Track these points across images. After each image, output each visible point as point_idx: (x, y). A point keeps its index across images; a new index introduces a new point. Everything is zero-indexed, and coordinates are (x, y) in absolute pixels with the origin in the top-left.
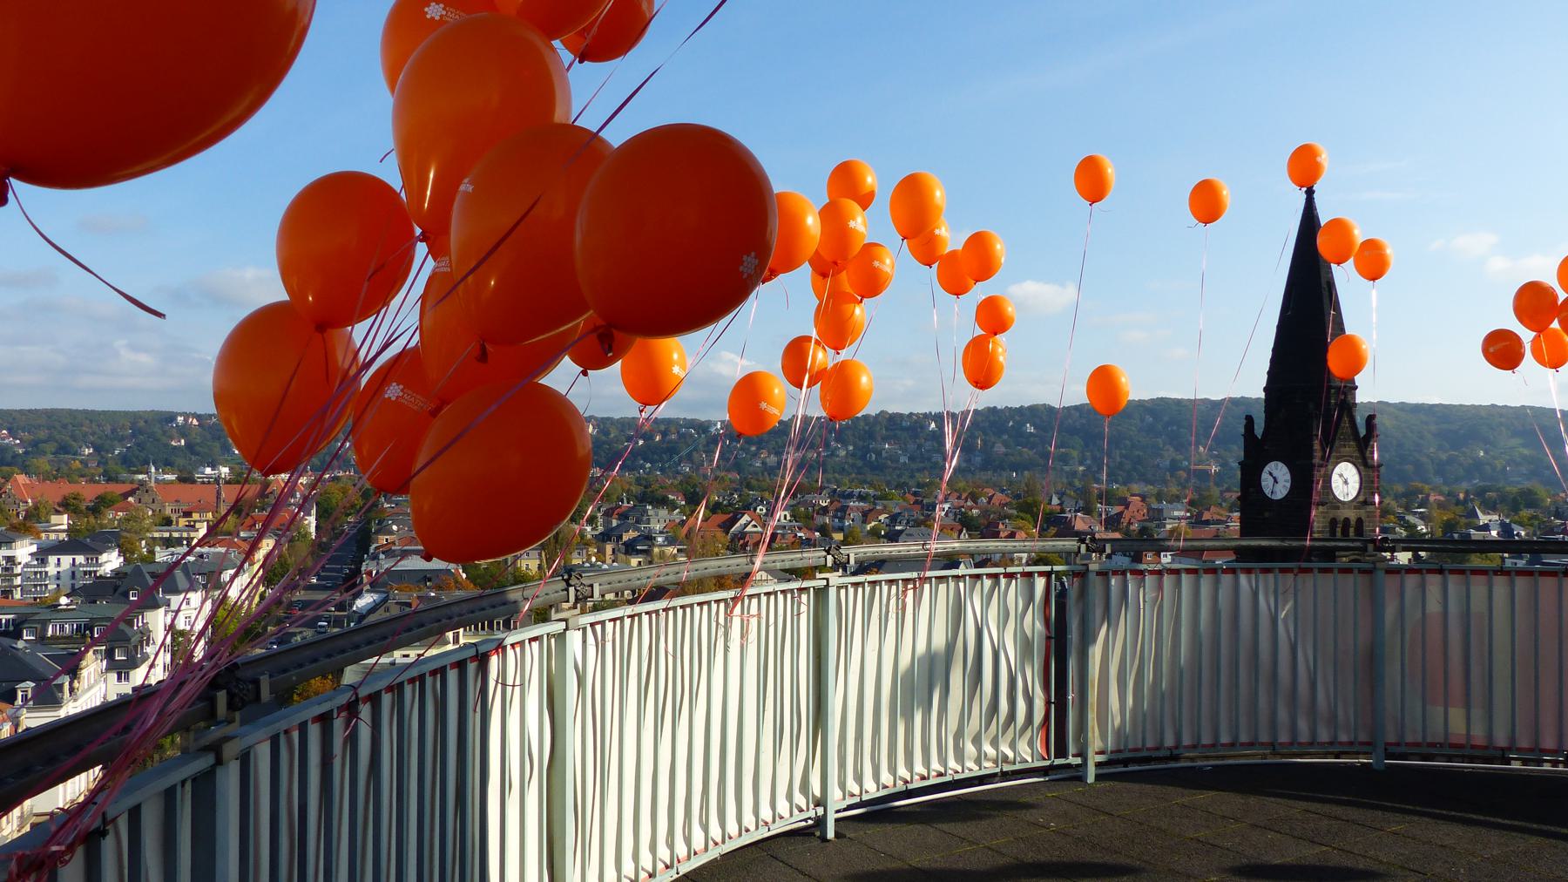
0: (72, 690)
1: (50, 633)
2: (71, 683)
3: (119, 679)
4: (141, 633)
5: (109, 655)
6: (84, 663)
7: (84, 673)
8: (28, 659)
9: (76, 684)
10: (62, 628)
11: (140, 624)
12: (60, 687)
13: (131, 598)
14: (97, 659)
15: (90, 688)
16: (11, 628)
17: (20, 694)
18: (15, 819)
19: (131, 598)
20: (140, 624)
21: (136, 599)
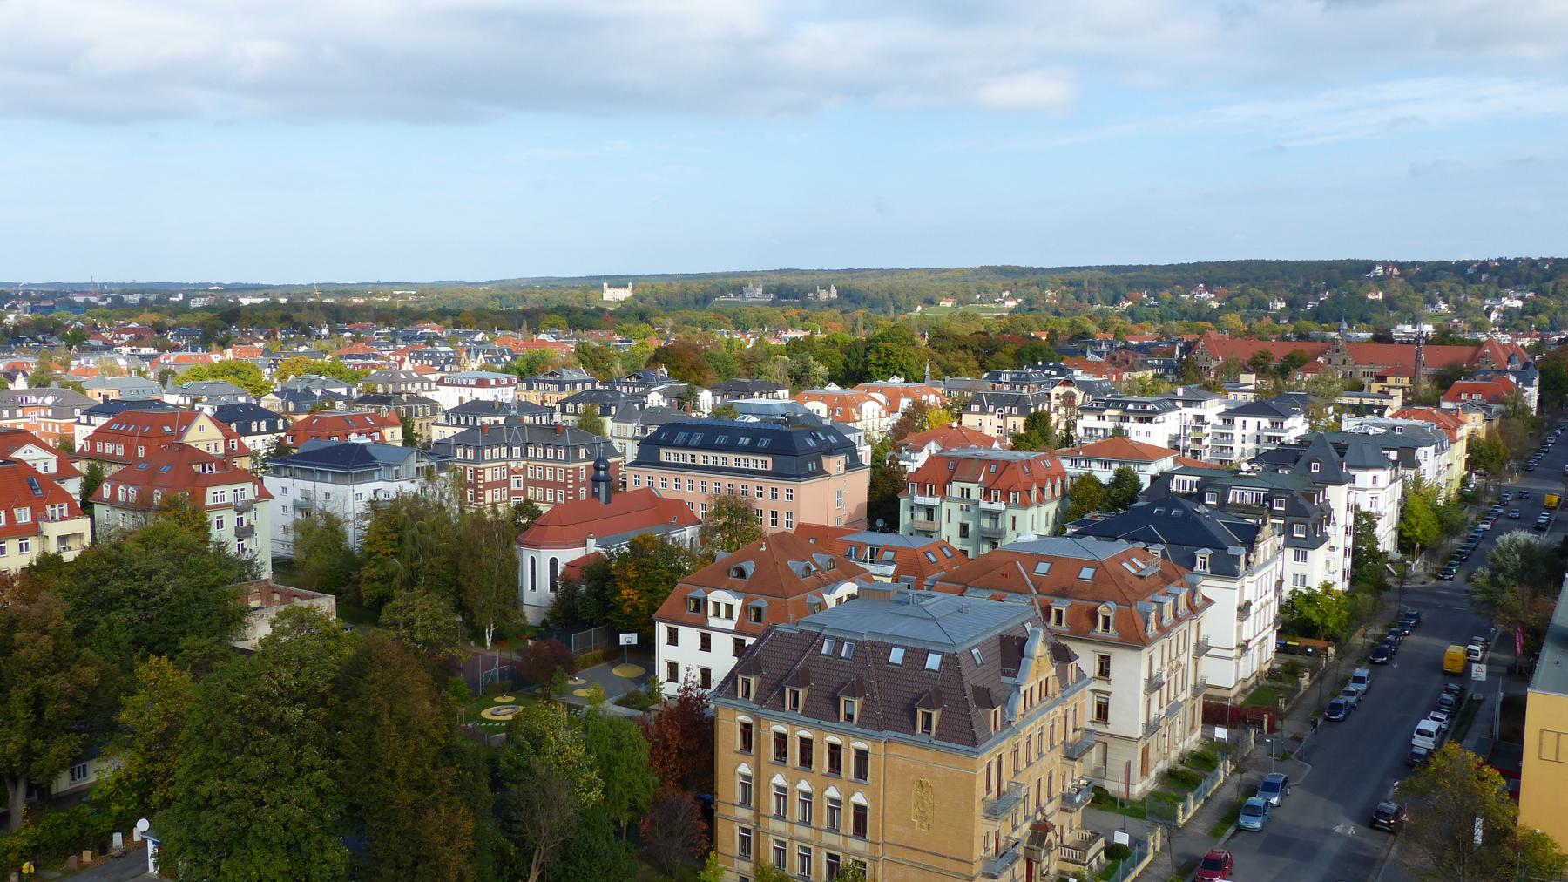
0: (1248, 562)
1: (1230, 499)
2: (1247, 556)
3: (1296, 558)
4: (1322, 510)
5: (1287, 530)
6: (1260, 536)
7: (1261, 547)
8: (1208, 525)
9: (1252, 558)
10: (1242, 497)
11: (1321, 501)
12: (1237, 558)
13: (1313, 471)
14: (1273, 534)
15: (1266, 563)
16: (1195, 490)
17: (1199, 560)
18: (1189, 687)
19: (1313, 471)
20: (1321, 501)
21: (1318, 471)
